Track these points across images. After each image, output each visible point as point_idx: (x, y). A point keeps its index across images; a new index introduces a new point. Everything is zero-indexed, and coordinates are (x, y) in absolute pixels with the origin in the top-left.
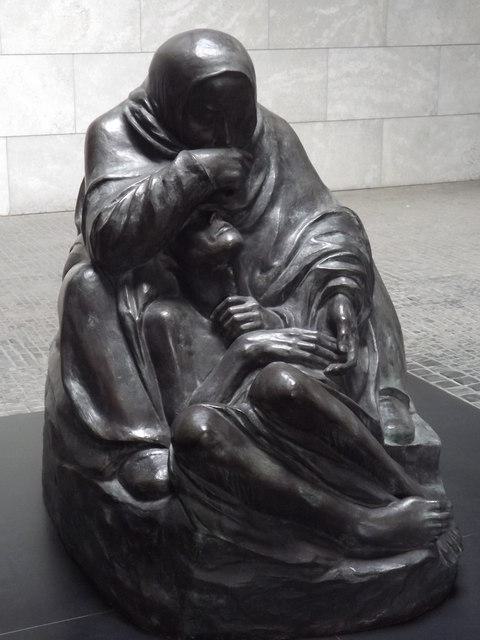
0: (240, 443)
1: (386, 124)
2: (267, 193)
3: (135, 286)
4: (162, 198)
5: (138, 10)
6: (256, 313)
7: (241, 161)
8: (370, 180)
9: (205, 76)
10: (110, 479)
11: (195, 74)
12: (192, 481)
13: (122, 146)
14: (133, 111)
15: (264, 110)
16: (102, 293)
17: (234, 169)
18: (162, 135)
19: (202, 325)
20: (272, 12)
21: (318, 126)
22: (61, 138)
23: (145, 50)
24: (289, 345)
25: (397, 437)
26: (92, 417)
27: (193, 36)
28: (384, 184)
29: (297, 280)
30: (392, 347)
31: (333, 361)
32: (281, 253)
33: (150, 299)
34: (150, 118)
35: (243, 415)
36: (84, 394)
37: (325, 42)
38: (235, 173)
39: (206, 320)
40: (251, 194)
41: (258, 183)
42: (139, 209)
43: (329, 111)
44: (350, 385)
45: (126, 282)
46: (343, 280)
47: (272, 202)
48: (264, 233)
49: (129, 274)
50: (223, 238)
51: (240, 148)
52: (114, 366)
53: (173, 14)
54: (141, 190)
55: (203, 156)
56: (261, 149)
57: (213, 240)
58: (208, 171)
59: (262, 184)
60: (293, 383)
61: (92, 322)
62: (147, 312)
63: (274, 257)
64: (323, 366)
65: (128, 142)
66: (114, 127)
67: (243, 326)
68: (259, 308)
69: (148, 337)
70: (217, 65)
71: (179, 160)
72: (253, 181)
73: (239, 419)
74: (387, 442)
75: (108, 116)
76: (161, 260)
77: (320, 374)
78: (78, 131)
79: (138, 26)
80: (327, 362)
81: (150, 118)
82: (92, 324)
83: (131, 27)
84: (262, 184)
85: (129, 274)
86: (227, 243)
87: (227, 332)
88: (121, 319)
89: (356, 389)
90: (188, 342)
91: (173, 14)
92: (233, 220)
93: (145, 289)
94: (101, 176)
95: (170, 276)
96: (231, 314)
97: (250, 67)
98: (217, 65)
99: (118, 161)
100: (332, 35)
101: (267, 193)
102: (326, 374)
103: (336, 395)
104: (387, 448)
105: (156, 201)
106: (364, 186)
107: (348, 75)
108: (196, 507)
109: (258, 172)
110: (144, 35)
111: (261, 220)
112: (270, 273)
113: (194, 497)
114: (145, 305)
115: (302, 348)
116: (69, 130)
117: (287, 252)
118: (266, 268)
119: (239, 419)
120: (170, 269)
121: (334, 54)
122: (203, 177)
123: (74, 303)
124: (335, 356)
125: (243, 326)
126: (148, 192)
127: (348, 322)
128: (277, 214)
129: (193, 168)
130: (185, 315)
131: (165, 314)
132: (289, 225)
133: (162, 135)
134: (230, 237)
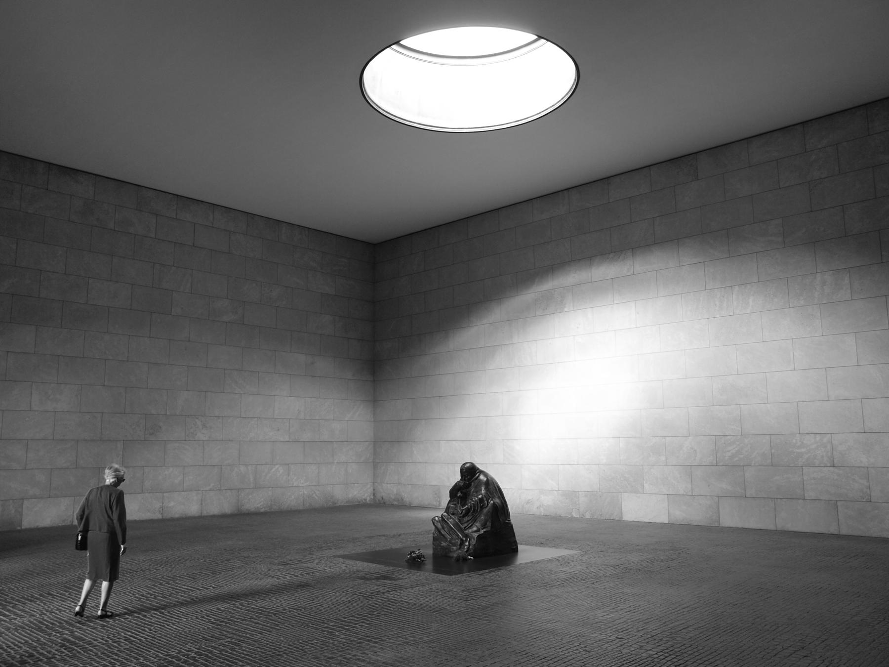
1: (839, 504)
8: (833, 530)
22: (687, 496)
28: (841, 533)
37: (800, 464)
53: (729, 451)
92: (462, 492)
106: (829, 533)
107: (814, 479)
116: (690, 494)
121: (805, 469)
134: (459, 495)
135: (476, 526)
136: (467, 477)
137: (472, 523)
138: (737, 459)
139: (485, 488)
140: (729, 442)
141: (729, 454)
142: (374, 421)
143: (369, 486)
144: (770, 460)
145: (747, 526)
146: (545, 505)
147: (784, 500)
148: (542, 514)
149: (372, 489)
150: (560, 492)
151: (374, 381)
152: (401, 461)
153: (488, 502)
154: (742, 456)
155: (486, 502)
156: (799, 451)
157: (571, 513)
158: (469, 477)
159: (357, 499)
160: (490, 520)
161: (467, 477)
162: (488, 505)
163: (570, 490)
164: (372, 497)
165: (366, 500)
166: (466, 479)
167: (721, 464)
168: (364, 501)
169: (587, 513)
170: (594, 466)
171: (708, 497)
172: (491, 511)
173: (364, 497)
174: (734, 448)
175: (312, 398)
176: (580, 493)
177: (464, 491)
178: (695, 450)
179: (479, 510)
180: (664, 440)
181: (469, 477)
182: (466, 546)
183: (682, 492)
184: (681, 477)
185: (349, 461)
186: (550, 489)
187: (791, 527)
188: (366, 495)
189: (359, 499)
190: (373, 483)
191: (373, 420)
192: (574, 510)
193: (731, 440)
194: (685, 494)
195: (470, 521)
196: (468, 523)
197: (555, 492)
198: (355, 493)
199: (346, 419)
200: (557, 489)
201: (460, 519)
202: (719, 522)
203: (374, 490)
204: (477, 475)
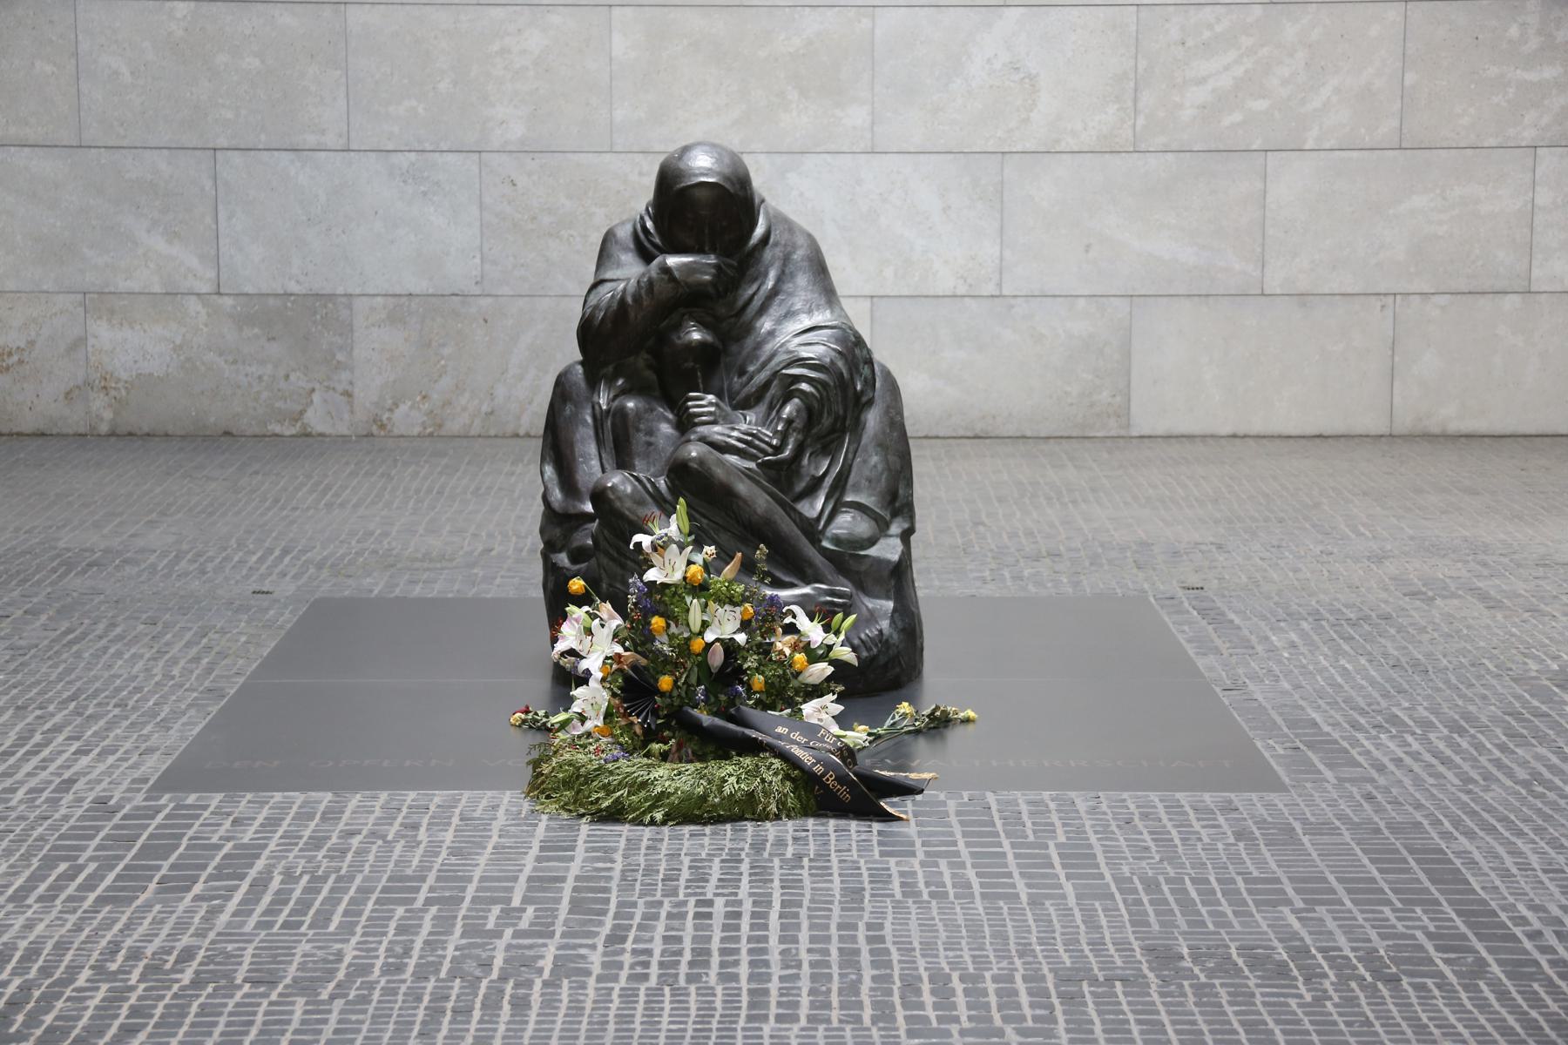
0: (641, 503)
2: (757, 303)
3: (610, 381)
4: (637, 298)
5: (1132, 76)
6: (712, 409)
7: (717, 267)
9: (683, 185)
10: (560, 551)
11: (676, 183)
12: (606, 539)
13: (626, 249)
14: (642, 218)
15: (779, 219)
16: (583, 384)
17: (707, 274)
18: (657, 240)
19: (668, 421)
20: (1410, 78)
21: (1511, 302)
23: (1143, 147)
24: (730, 437)
25: (837, 540)
26: (557, 495)
27: (686, 149)
29: (766, 385)
30: (875, 466)
31: (767, 454)
32: (757, 359)
33: (625, 392)
34: (649, 224)
35: (653, 484)
36: (555, 477)
37: (1528, 135)
38: (707, 277)
39: (670, 416)
40: (740, 303)
41: (750, 292)
42: (615, 305)
43: (1536, 273)
45: (605, 376)
46: (804, 386)
47: (763, 310)
48: (749, 342)
49: (610, 369)
50: (687, 338)
51: (724, 252)
52: (578, 449)
53: (1202, 81)
54: (622, 286)
55: (673, 261)
56: (758, 261)
57: (679, 338)
58: (676, 274)
59: (754, 294)
60: (694, 454)
61: (568, 409)
62: (616, 403)
63: (752, 362)
64: (753, 458)
65: (632, 246)
66: (624, 233)
67: (696, 420)
68: (716, 405)
69: (613, 424)
70: (696, 175)
71: (656, 262)
72: (745, 290)
73: (649, 486)
74: (826, 544)
75: (623, 223)
76: (641, 360)
77: (752, 465)
78: (1005, 292)
79: (1130, 104)
80: (761, 455)
81: (649, 224)
82: (568, 412)
83: (1116, 106)
84: (754, 294)
85: (610, 369)
86: (691, 342)
87: (685, 424)
88: (594, 406)
89: (800, 486)
90: (650, 433)
91: (1202, 81)
92: (703, 324)
93: (620, 382)
94: (602, 277)
95: (650, 375)
96: (688, 408)
97: (743, 182)
98: (696, 175)
99: (619, 265)
100: (1545, 120)
101: (757, 303)
102: (758, 465)
103: (757, 483)
104: (825, 552)
105: (629, 300)
108: (605, 561)
109: (755, 279)
110: (1141, 121)
111: (749, 328)
112: (744, 379)
113: (607, 554)
114: (616, 397)
115: (739, 440)
116: (990, 289)
117: (762, 359)
118: (742, 372)
119: (649, 486)
120: (649, 367)
122: (672, 279)
123: (562, 391)
124: (770, 450)
125: (696, 420)
126: (624, 290)
127: (789, 422)
128: (766, 324)
129: (666, 270)
130: (652, 410)
131: (631, 405)
132: (771, 333)
133: (657, 240)
134: (696, 336)
135: (858, 506)
138: (1237, 117)
140: (1207, 34)
141: (1199, 95)
144: (1395, 123)
145: (1257, 427)
146: (124, 376)
147: (1442, 300)
148: (104, 428)
150: (228, 302)
154: (1260, 105)
156: (1532, 76)
157: (302, 413)
163: (294, 287)
167: (1159, 141)
169: (403, 408)
170: (450, 157)
171: (1082, 302)
174: (1226, 68)
176: (359, 304)
178: (1032, 78)
180: (866, 23)
183: (945, 282)
184: (946, 209)
186: (157, 289)
187: (1450, 417)
192: (316, 397)
193: (1218, 29)
194: (962, 290)
197: (193, 305)
200: (205, 288)
202: (1123, 413)
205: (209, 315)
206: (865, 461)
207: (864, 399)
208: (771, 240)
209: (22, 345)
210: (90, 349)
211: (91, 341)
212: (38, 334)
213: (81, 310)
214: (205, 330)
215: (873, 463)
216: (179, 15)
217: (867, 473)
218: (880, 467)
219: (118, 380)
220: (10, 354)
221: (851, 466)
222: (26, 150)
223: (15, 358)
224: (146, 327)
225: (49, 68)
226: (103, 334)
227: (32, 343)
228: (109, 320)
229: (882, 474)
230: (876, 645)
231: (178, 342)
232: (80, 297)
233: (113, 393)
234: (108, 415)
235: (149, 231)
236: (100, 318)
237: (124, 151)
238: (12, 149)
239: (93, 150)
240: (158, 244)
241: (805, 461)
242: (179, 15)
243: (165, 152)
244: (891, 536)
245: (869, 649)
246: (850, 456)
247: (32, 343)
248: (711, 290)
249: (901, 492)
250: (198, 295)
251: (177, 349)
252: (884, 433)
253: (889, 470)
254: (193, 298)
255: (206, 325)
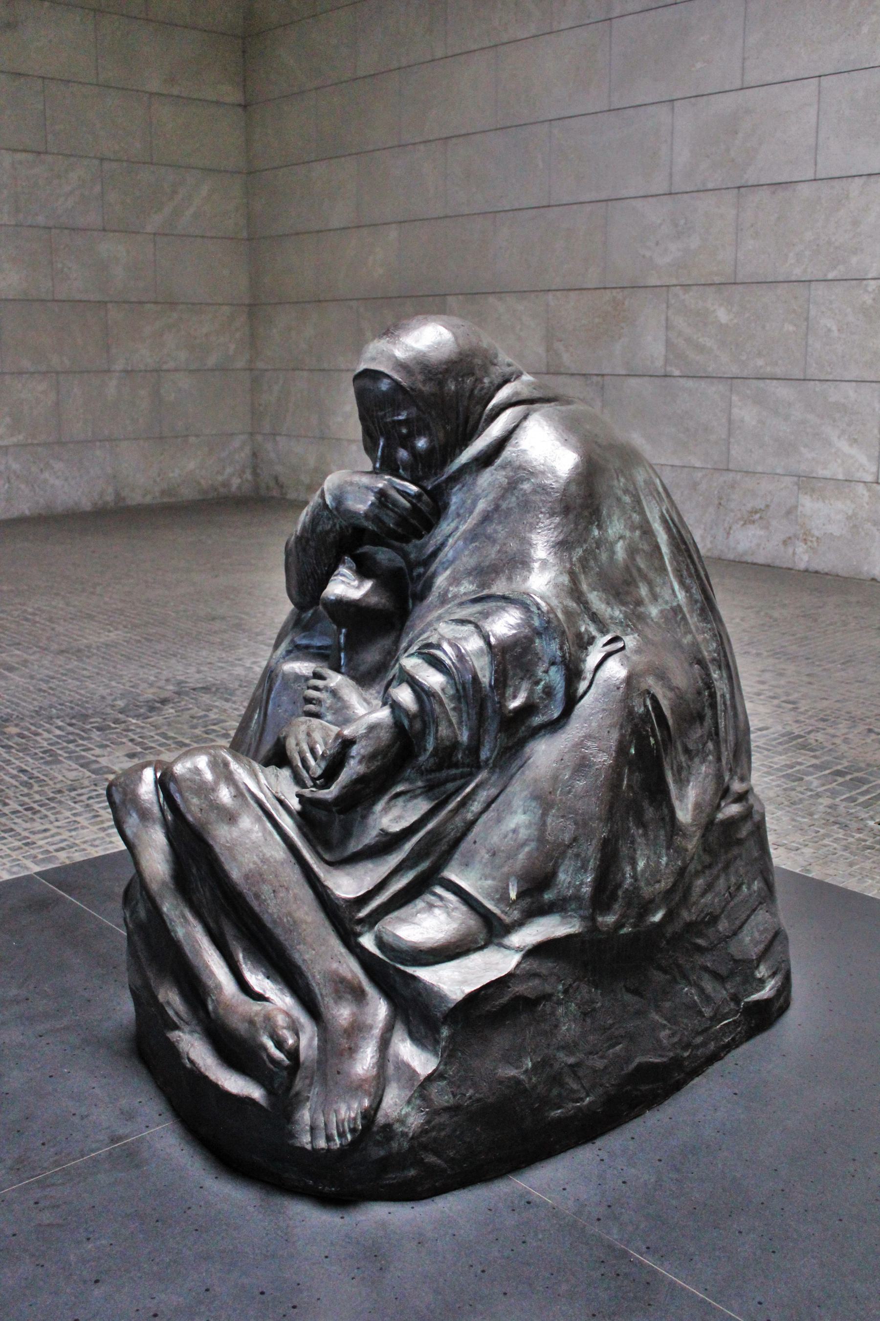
30: (515, 831)
44: (347, 834)
74: (368, 941)
92: (363, 571)
136: (407, 442)
137: (424, 865)
139: (563, 546)
142: (249, 239)
143: (237, 443)
148: (802, 566)
149: (247, 450)
151: (245, 107)
152: (325, 366)
153: (573, 673)
155: (556, 677)
158: (422, 443)
159: (199, 483)
160: (591, 850)
161: (407, 442)
162: (571, 701)
164: (248, 476)
165: (226, 484)
166: (403, 454)
168: (222, 490)
172: (603, 759)
173: (220, 478)
175: (16, 151)
177: (384, 556)
179: (484, 754)
181: (422, 443)
182: (356, 1088)
185: (165, 367)
188: (229, 470)
189: (203, 482)
190: (251, 434)
191: (245, 234)
195: (408, 846)
196: (394, 860)
197: (861, 489)
198: (192, 465)
199: (149, 229)
200: (869, 478)
201: (321, 815)
203: (254, 455)
204: (496, 430)
205: (870, 497)
206: (499, 820)
207: (537, 720)
208: (498, 462)
209: (762, 507)
210: (799, 513)
211: (800, 509)
212: (772, 501)
213: (796, 487)
214: (867, 507)
215: (512, 826)
216: (870, 289)
217: (495, 839)
218: (523, 834)
219: (813, 536)
220: (756, 512)
221: (471, 824)
222: (775, 381)
223: (758, 516)
224: (832, 502)
225: (791, 328)
226: (808, 504)
227: (767, 506)
228: (811, 496)
229: (523, 845)
230: (342, 1135)
231: (850, 513)
232: (796, 479)
233: (809, 544)
234: (806, 558)
235: (839, 437)
236: (806, 493)
237: (829, 383)
238: (768, 381)
239: (812, 383)
240: (843, 445)
241: (379, 807)
242: (870, 289)
243: (854, 384)
244: (507, 948)
245: (329, 1138)
246: (476, 807)
247: (767, 506)
248: (370, 526)
249: (563, 877)
250: (865, 482)
251: (849, 518)
252: (555, 778)
253: (541, 839)
254: (862, 485)
255: (868, 504)
